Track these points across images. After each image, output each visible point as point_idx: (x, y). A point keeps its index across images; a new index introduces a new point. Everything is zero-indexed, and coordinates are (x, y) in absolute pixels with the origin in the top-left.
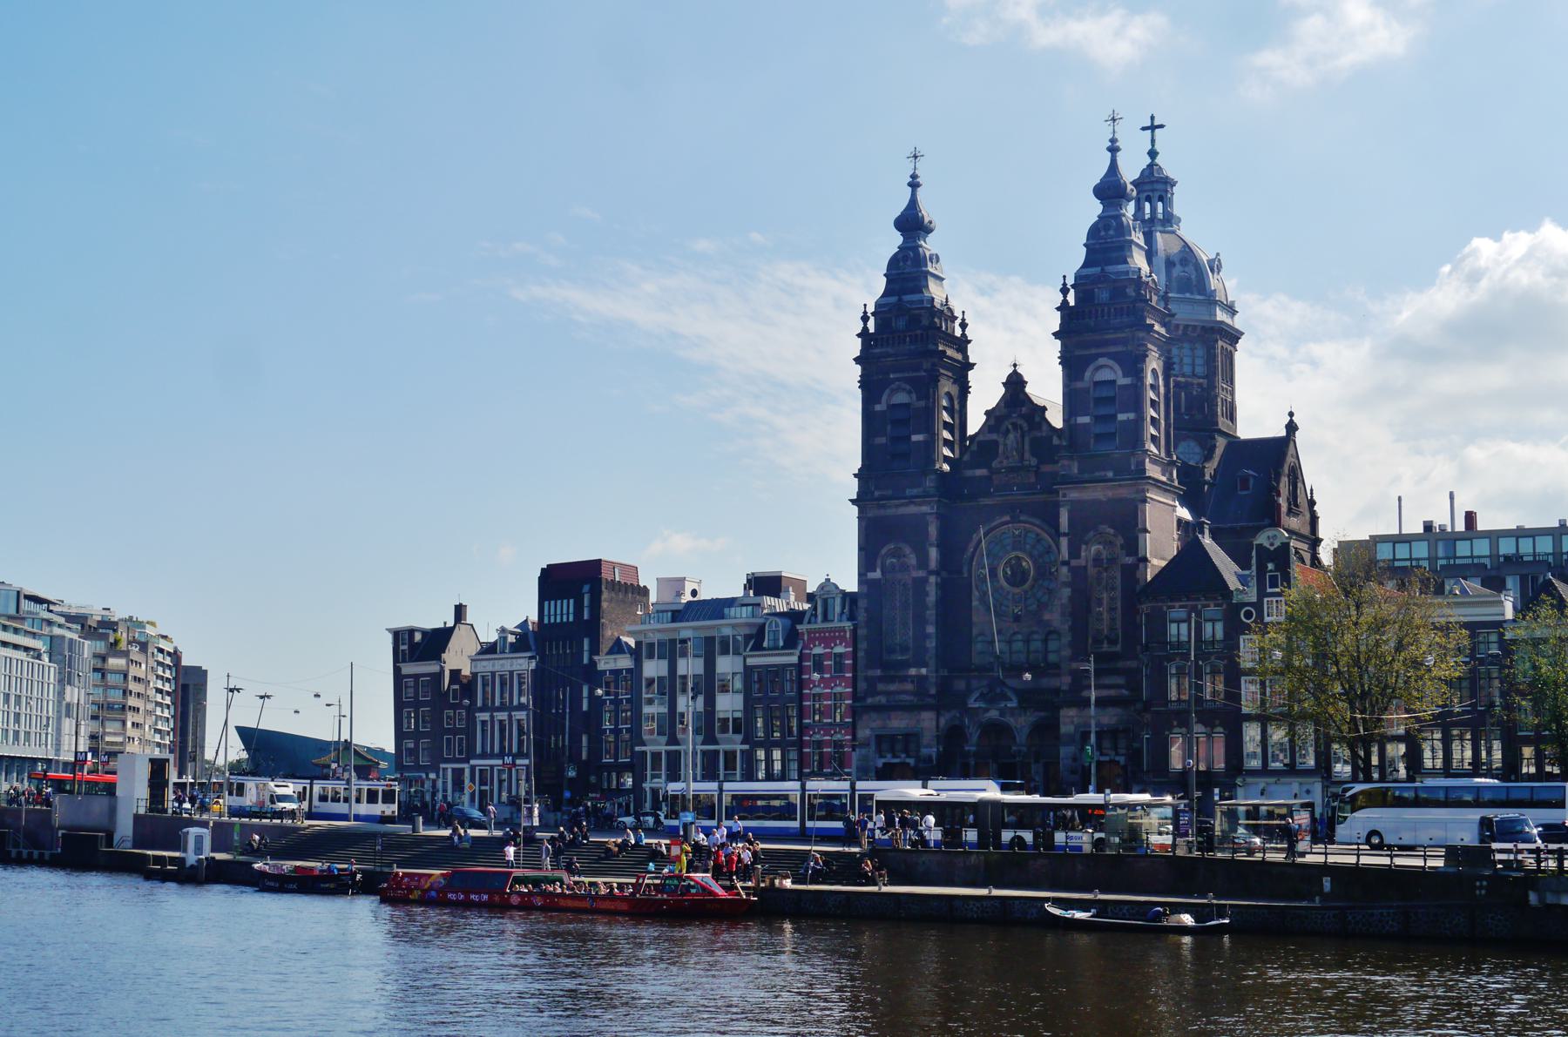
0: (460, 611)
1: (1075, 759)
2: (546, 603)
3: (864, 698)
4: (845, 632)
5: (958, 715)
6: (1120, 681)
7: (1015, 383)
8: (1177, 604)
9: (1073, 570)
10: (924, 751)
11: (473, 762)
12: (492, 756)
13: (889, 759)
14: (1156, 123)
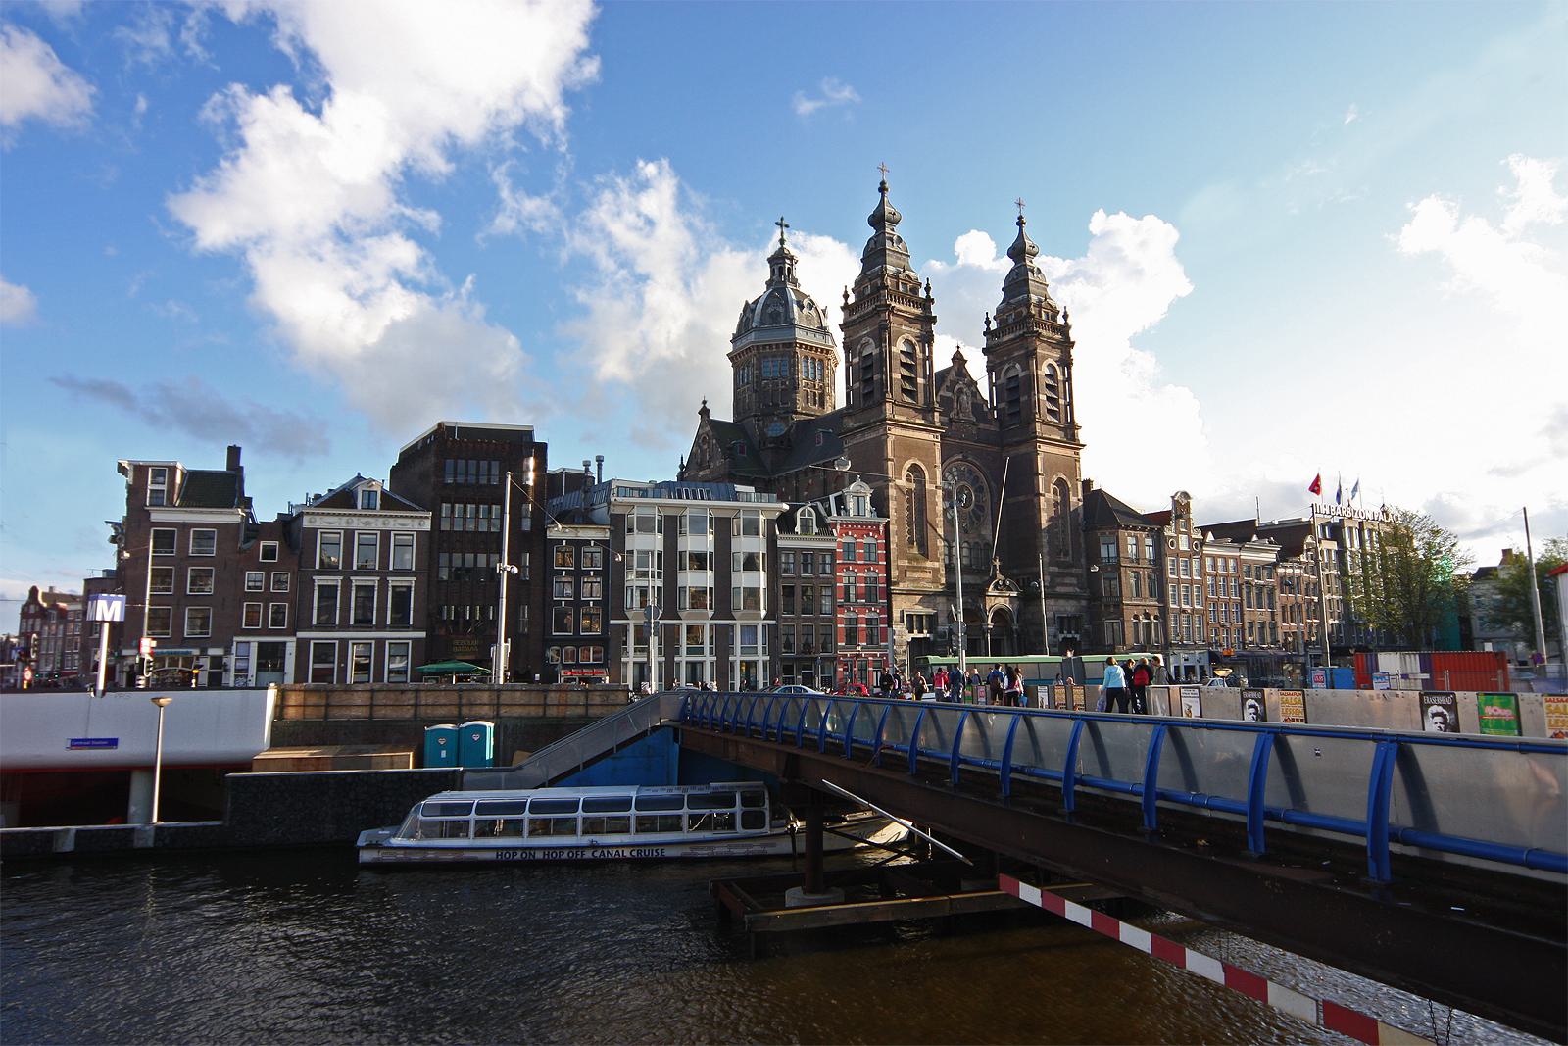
0: (234, 453)
1: (1055, 636)
2: (450, 462)
3: (896, 584)
4: (878, 526)
5: (970, 600)
6: (1074, 581)
7: (959, 359)
8: (1132, 533)
9: (1047, 501)
10: (940, 629)
11: (300, 635)
12: (330, 627)
13: (916, 635)
14: (785, 222)
